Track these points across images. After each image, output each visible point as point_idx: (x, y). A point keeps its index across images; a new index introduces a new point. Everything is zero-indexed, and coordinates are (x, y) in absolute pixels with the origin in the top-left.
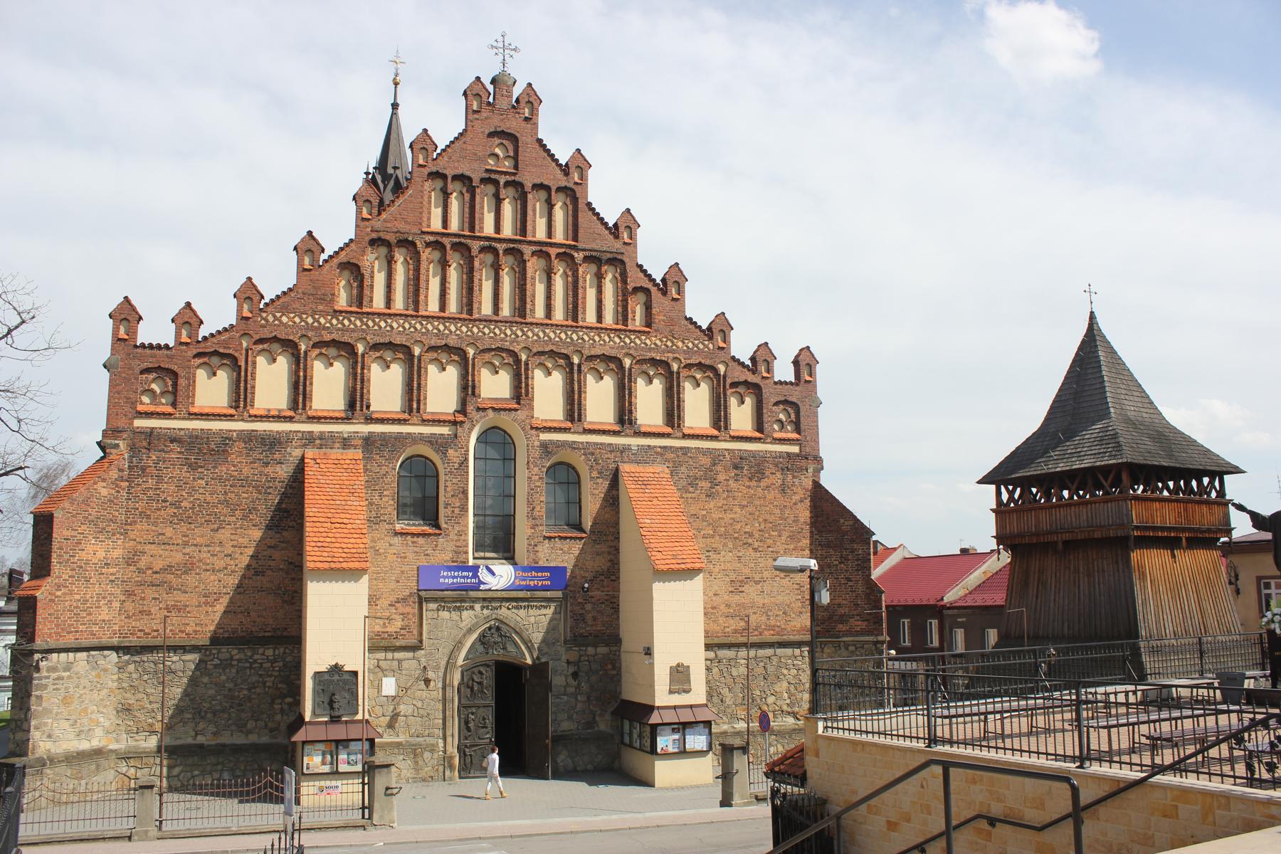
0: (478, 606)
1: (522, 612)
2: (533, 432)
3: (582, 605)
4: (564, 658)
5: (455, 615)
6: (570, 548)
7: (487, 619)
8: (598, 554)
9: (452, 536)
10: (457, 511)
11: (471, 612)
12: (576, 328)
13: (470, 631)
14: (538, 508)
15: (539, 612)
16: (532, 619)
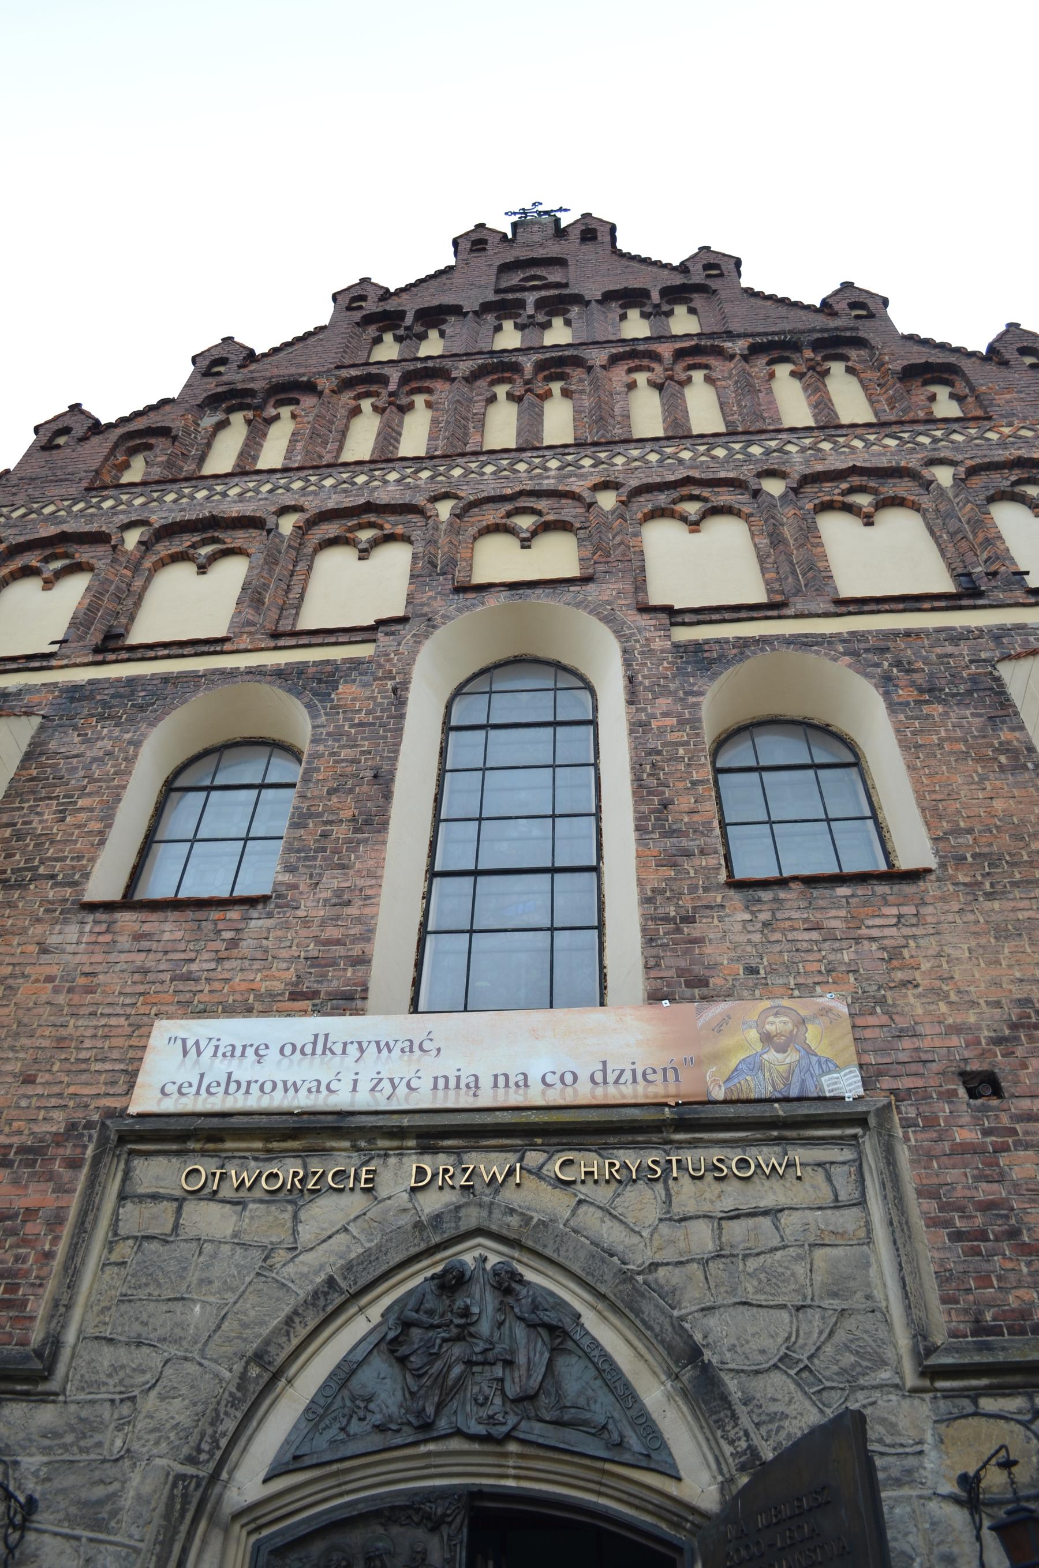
0: (399, 1173)
1: (642, 1203)
2: (644, 621)
3: (987, 1158)
4: (940, 1468)
5: (266, 1224)
6: (855, 921)
7: (437, 1235)
8: (1001, 933)
9: (310, 906)
10: (341, 832)
11: (356, 1202)
12: (751, 435)
13: (333, 1300)
14: (684, 802)
15: (733, 1196)
16: (701, 1237)
